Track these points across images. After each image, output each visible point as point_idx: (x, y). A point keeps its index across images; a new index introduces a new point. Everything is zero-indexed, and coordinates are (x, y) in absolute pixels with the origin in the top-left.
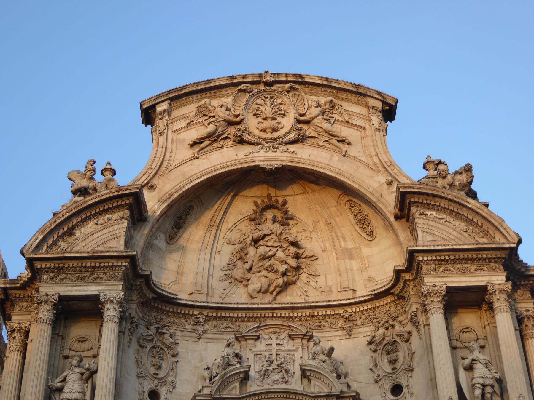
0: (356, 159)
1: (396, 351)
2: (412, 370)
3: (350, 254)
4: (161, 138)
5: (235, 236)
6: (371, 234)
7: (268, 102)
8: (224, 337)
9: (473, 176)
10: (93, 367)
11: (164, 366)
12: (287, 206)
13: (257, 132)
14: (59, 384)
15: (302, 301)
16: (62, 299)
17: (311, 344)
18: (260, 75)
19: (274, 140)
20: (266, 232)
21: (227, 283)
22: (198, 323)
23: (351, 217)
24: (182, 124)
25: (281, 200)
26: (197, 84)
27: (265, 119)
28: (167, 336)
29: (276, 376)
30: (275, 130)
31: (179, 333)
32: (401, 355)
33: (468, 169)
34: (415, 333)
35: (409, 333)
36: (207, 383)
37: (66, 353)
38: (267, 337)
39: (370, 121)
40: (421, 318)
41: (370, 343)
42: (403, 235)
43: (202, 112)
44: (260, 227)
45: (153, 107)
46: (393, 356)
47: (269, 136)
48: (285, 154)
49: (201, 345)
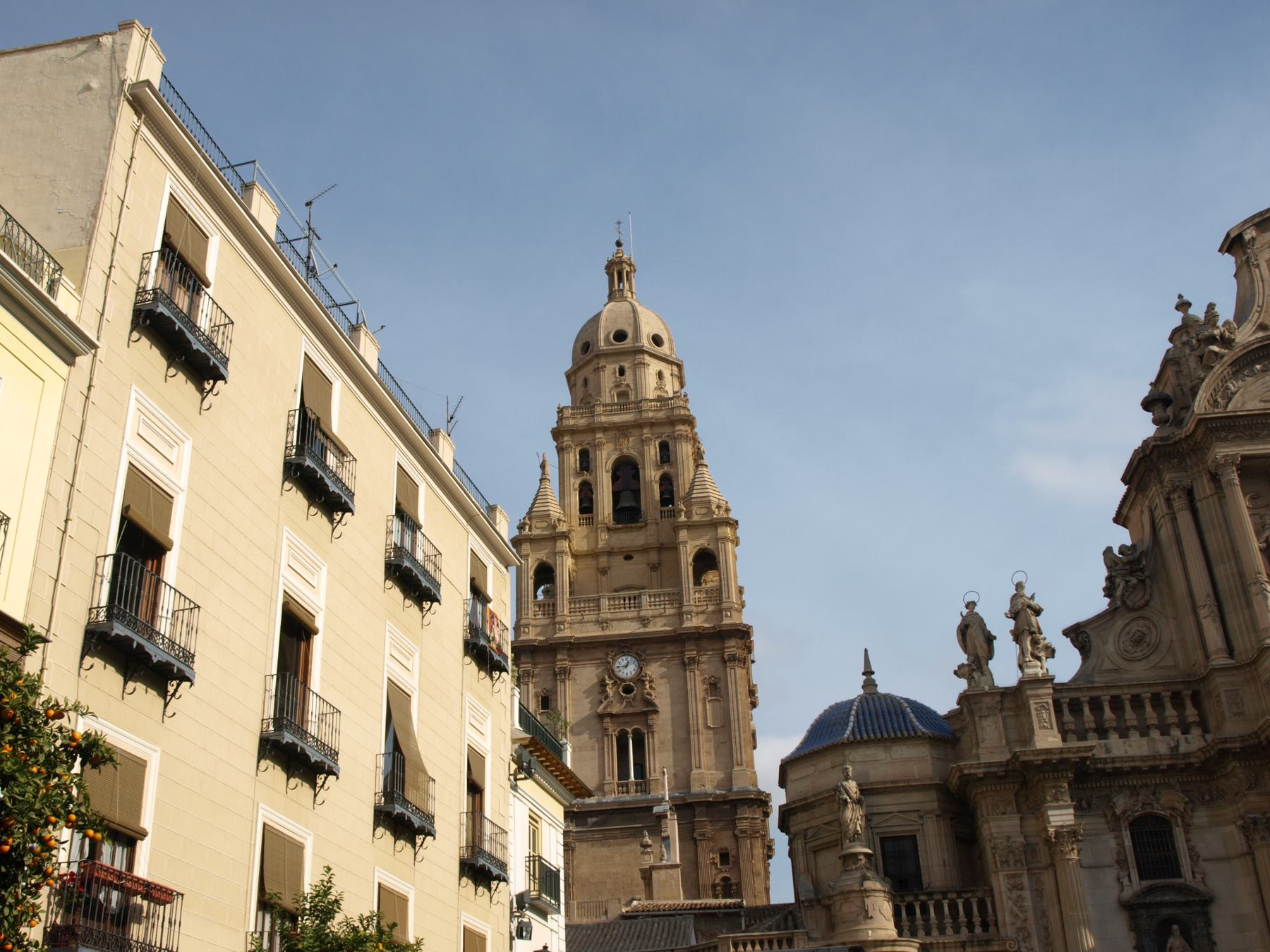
16: (1244, 458)
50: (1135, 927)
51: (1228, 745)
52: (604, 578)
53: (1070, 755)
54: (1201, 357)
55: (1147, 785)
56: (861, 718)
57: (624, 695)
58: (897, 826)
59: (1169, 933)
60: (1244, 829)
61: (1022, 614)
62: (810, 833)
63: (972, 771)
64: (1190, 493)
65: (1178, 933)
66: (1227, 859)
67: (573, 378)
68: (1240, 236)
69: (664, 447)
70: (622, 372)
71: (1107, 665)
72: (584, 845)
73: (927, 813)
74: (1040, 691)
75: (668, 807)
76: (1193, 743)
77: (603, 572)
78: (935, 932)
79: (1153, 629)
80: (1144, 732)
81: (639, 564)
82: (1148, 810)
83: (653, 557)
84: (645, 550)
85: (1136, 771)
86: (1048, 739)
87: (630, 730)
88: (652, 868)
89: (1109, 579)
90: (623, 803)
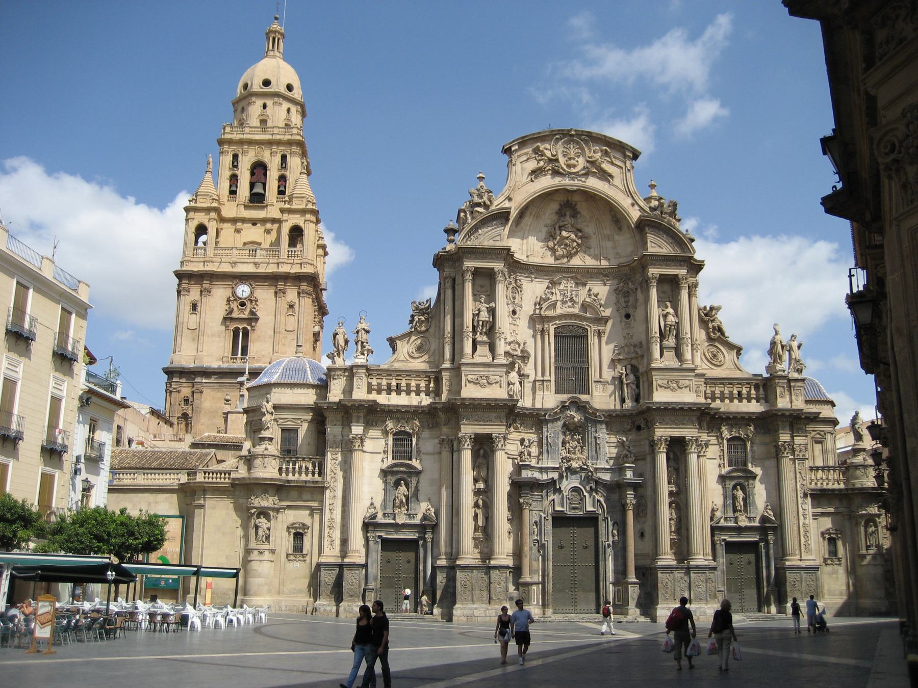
0: (617, 187)
1: (628, 296)
2: (636, 308)
3: (609, 238)
4: (514, 167)
5: (549, 222)
6: (620, 229)
7: (572, 147)
8: (544, 280)
9: (676, 209)
10: (494, 305)
11: (517, 297)
12: (577, 207)
13: (565, 167)
14: (477, 312)
15: (584, 264)
16: (476, 268)
17: (587, 287)
18: (568, 130)
19: (574, 173)
20: (566, 223)
21: (544, 249)
22: (531, 273)
23: (611, 217)
24: (525, 158)
25: (574, 203)
26: (534, 134)
27: (570, 159)
28: (518, 281)
29: (570, 304)
30: (574, 166)
31: (523, 278)
32: (631, 299)
33: (675, 205)
34: (639, 290)
35: (636, 289)
36: (538, 307)
37: (476, 293)
38: (565, 282)
39: (625, 164)
40: (644, 285)
41: (615, 290)
42: (638, 237)
43: (536, 151)
44: (562, 219)
45: (510, 148)
46: (626, 299)
47: (573, 170)
48: (580, 182)
49: (534, 284)
50: (385, 482)
51: (437, 405)
52: (238, 235)
53: (364, 403)
54: (472, 212)
55: (404, 418)
56: (285, 371)
57: (240, 307)
58: (290, 425)
59: (400, 485)
60: (440, 443)
61: (360, 333)
62: (253, 423)
63: (322, 405)
64: (454, 280)
65: (403, 485)
66: (433, 454)
67: (236, 106)
68: (510, 148)
69: (284, 158)
70: (265, 106)
71: (402, 358)
72: (208, 390)
73: (304, 420)
74: (359, 371)
75: (246, 379)
76: (426, 401)
77: (238, 231)
78: (297, 475)
79: (428, 343)
80: (408, 393)
81: (259, 229)
82: (403, 429)
83: (269, 226)
84: (264, 221)
85: (398, 411)
86: (360, 394)
87: (241, 327)
88: (229, 413)
89: (413, 316)
90: (232, 369)
